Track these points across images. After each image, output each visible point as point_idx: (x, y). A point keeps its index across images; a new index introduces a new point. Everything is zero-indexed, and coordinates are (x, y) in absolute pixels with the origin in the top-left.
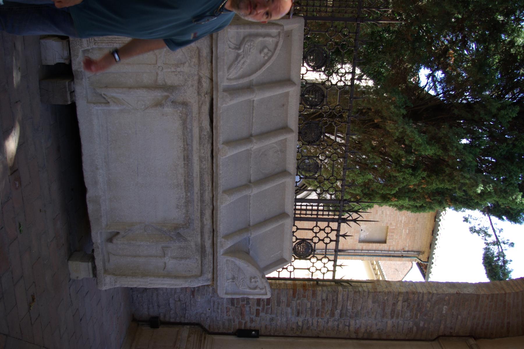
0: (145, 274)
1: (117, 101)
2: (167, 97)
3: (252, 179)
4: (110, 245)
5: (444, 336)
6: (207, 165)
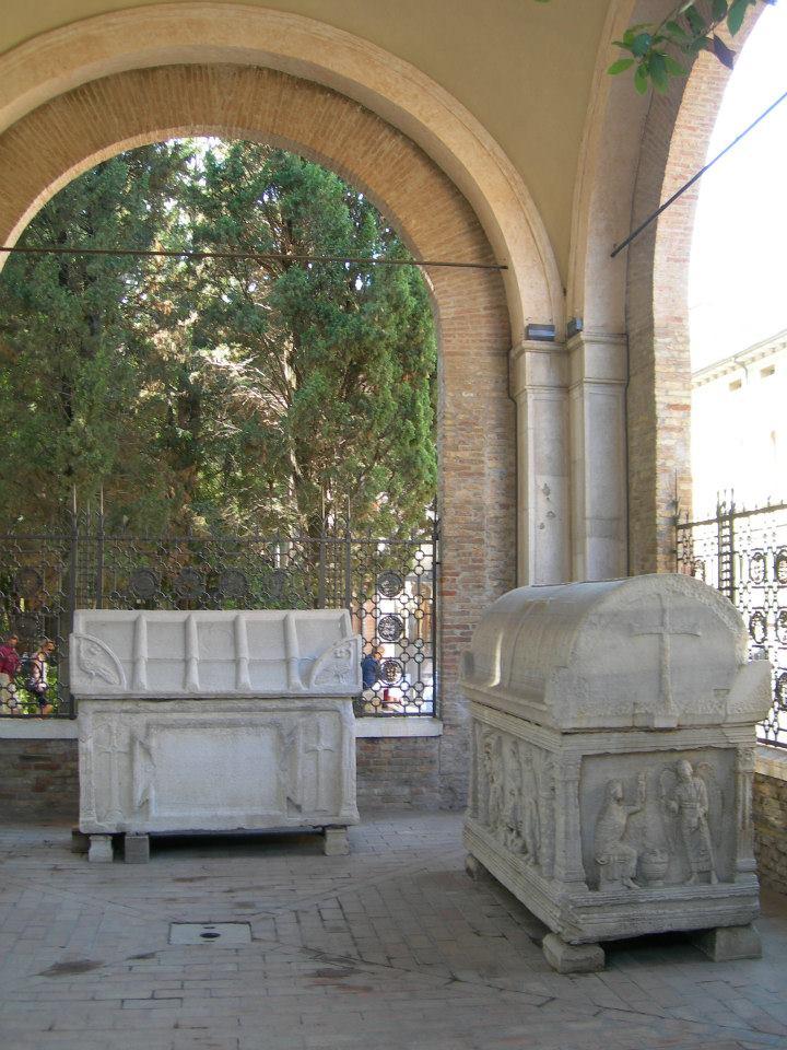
1: (146, 792)
2: (141, 744)
3: (231, 657)
4: (305, 808)
5: (508, 389)
6: (210, 705)
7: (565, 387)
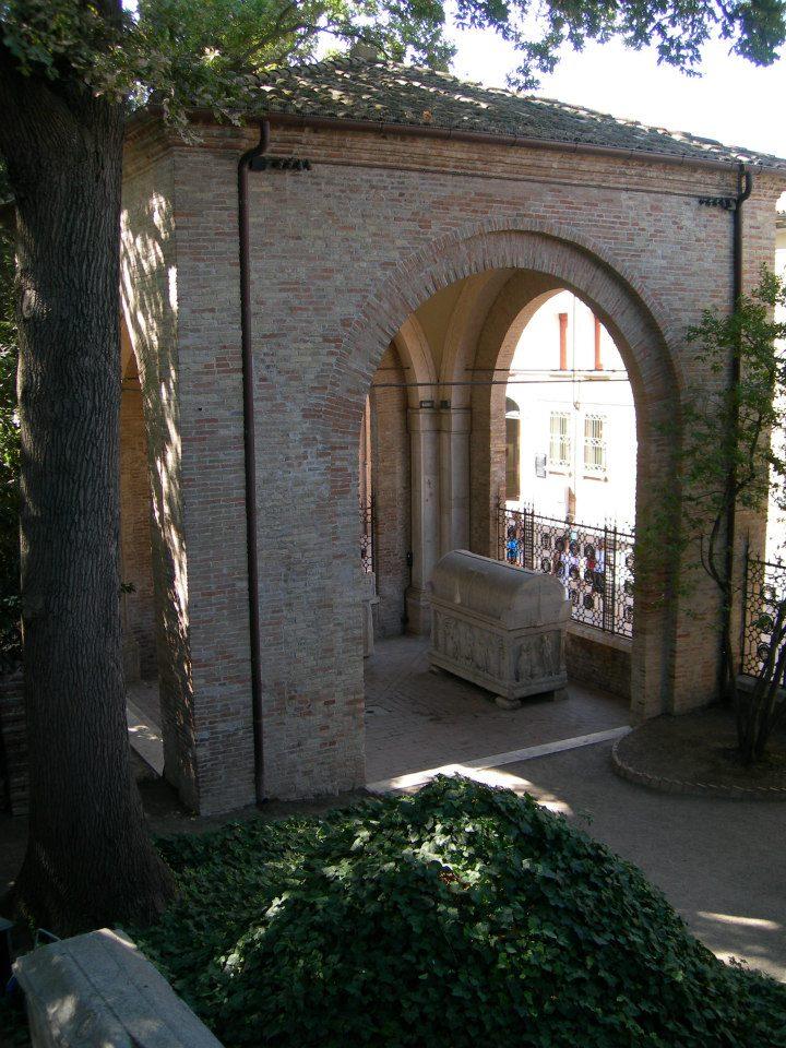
7: (438, 431)
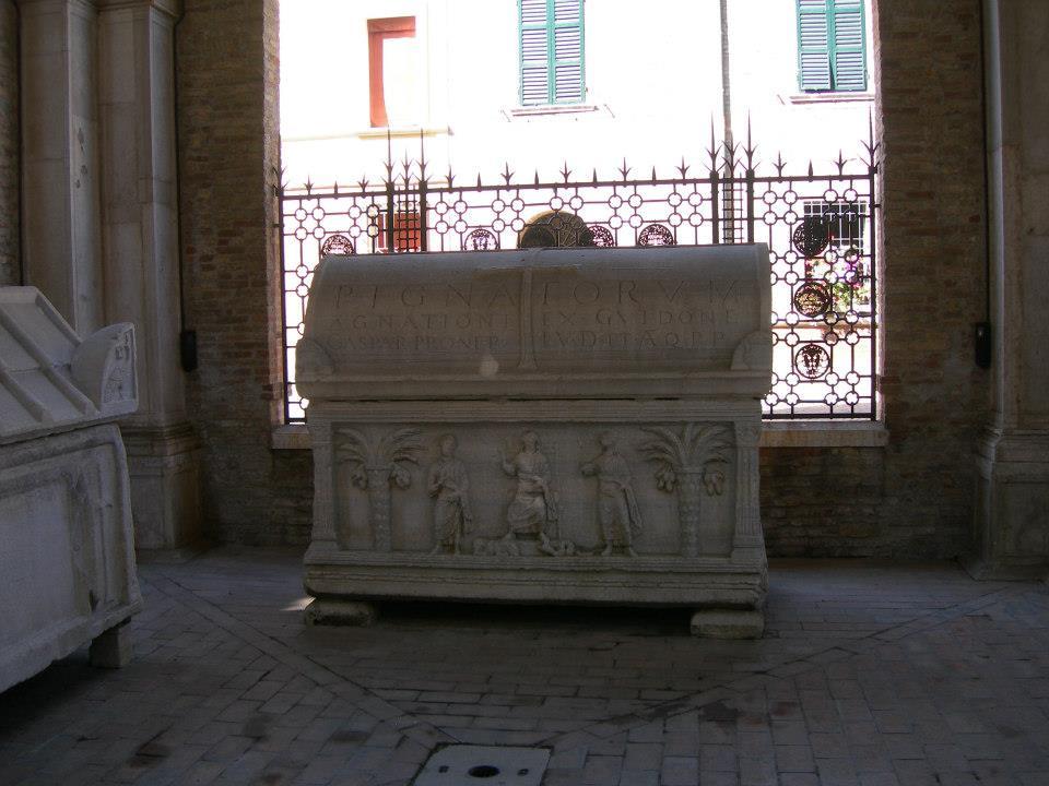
0: (120, 537)
